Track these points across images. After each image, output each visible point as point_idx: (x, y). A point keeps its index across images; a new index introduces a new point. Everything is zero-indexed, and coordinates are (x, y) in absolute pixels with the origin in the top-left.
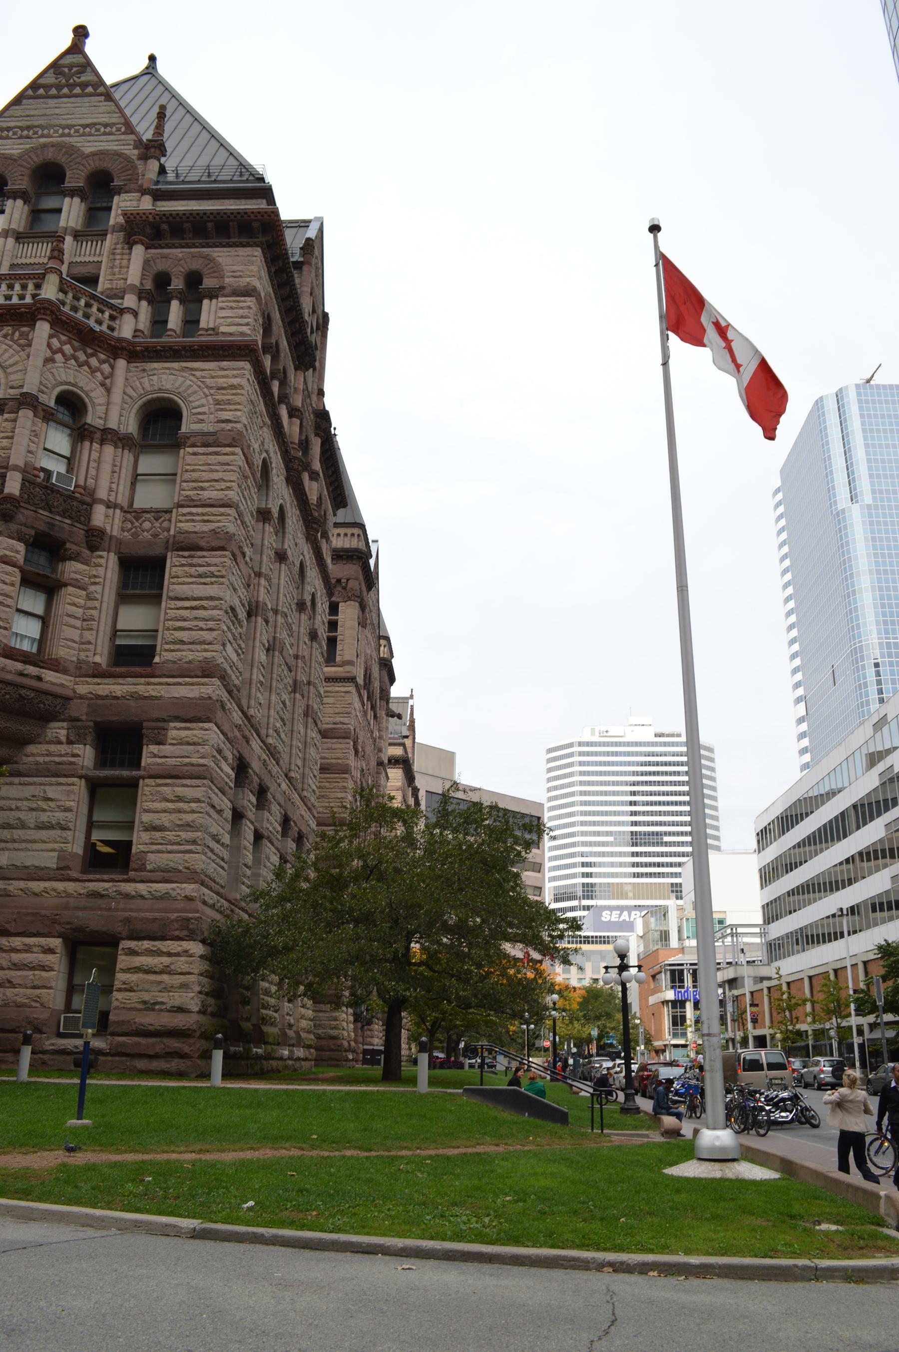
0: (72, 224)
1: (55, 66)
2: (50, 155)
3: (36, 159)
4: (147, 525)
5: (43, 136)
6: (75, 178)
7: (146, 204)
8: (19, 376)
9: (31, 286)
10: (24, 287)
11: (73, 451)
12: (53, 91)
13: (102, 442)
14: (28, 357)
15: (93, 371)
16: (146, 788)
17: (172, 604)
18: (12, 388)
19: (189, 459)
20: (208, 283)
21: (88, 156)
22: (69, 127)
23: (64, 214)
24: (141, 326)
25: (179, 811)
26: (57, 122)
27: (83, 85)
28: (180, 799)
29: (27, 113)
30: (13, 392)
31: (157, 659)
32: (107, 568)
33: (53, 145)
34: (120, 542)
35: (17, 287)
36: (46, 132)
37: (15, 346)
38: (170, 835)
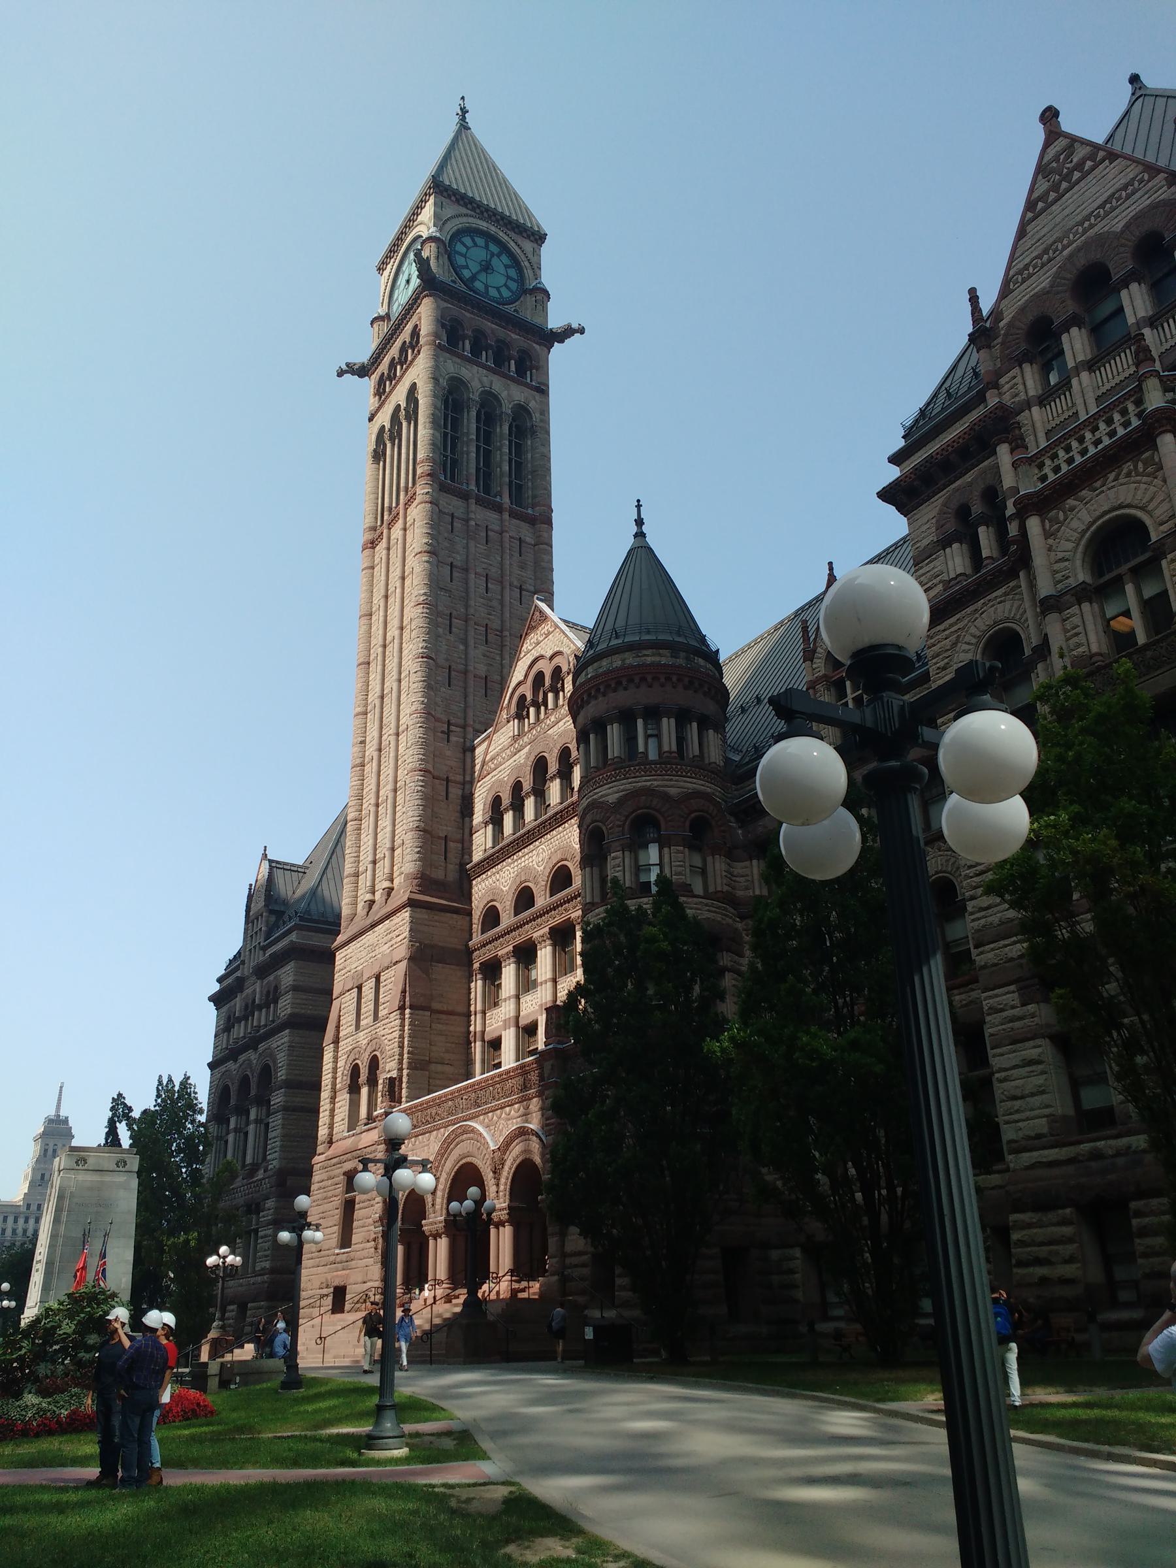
0: (1141, 313)
1: (1041, 170)
2: (1082, 262)
3: (1069, 276)
5: (1065, 248)
6: (1120, 263)
8: (1165, 506)
9: (1131, 407)
10: (1124, 412)
12: (1053, 195)
14: (1165, 481)
18: (1161, 524)
21: (1122, 232)
22: (1087, 218)
23: (1128, 311)
26: (1072, 223)
29: (1037, 237)
30: (1164, 528)
33: (1079, 249)
35: (1117, 417)
36: (1065, 242)
37: (1145, 479)
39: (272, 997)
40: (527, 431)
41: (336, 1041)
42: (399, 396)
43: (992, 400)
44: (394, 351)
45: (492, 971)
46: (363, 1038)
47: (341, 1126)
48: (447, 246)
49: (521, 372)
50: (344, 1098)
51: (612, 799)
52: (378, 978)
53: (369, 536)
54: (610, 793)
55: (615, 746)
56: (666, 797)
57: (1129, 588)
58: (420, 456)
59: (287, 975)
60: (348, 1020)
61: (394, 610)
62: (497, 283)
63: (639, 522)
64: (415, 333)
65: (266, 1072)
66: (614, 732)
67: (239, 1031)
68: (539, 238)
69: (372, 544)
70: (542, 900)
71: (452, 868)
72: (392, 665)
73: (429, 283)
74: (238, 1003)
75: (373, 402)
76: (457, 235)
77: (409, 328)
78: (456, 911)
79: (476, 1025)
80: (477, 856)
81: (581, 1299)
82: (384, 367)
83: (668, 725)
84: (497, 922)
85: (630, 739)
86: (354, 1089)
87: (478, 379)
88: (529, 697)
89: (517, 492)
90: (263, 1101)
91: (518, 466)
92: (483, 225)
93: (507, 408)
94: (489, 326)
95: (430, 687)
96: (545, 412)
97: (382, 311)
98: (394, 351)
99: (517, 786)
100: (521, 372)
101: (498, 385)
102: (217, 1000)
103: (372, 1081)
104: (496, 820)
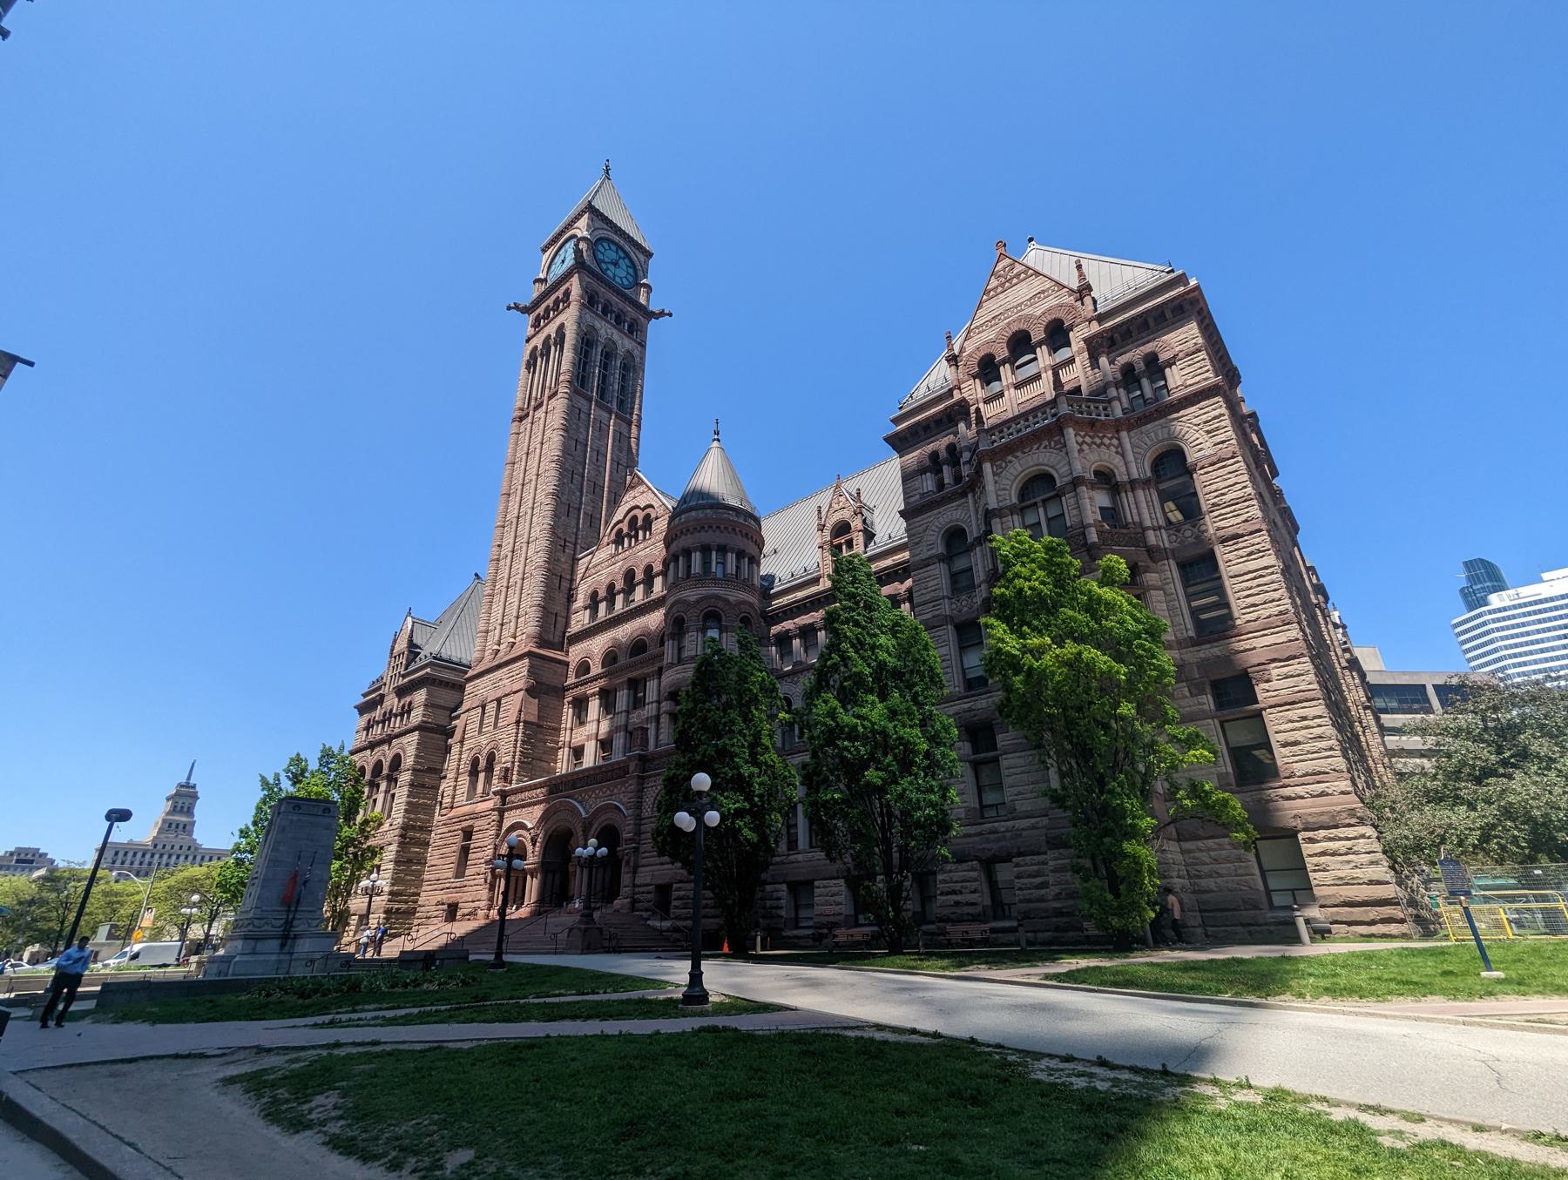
2: (1015, 328)
4: (1188, 533)
6: (1037, 334)
7: (1095, 327)
11: (1114, 501)
13: (1133, 490)
15: (1108, 447)
16: (1270, 717)
17: (1234, 580)
19: (1203, 478)
20: (1163, 357)
24: (1126, 405)
25: (1307, 727)
27: (1018, 275)
28: (1304, 718)
31: (1238, 622)
32: (1171, 571)
34: (1173, 551)
38: (1307, 747)
39: (407, 711)
40: (632, 368)
41: (462, 742)
42: (551, 329)
43: (957, 396)
44: (550, 302)
45: (580, 705)
46: (484, 740)
47: (461, 798)
48: (594, 245)
49: (631, 332)
50: (465, 780)
51: (693, 599)
52: (499, 701)
53: (519, 413)
54: (691, 594)
55: (696, 567)
56: (727, 601)
57: (1041, 510)
58: (563, 368)
59: (420, 696)
60: (473, 727)
61: (533, 463)
62: (620, 274)
63: (717, 433)
64: (567, 293)
65: (396, 762)
66: (697, 558)
67: (377, 731)
68: (649, 255)
69: (521, 419)
70: (622, 661)
71: (558, 633)
72: (529, 498)
73: (580, 265)
74: (378, 714)
75: (530, 331)
76: (600, 240)
77: (563, 289)
78: (560, 662)
79: (564, 737)
80: (574, 628)
81: (645, 914)
82: (541, 310)
83: (731, 558)
84: (588, 670)
85: (706, 564)
86: (474, 773)
87: (605, 330)
88: (625, 530)
89: (621, 403)
90: (392, 780)
91: (623, 388)
92: (616, 238)
93: (621, 351)
94: (614, 299)
95: (556, 515)
96: (643, 358)
97: (542, 276)
98: (550, 302)
99: (611, 587)
100: (631, 332)
101: (616, 336)
102: (363, 709)
103: (489, 769)
104: (593, 605)
